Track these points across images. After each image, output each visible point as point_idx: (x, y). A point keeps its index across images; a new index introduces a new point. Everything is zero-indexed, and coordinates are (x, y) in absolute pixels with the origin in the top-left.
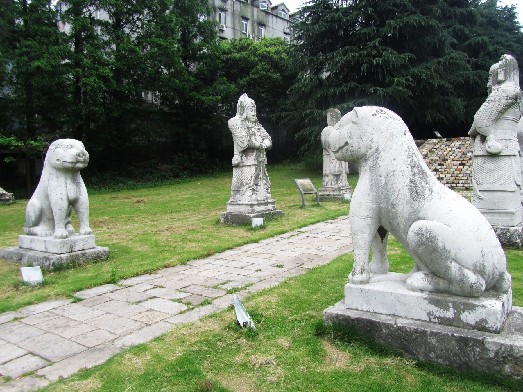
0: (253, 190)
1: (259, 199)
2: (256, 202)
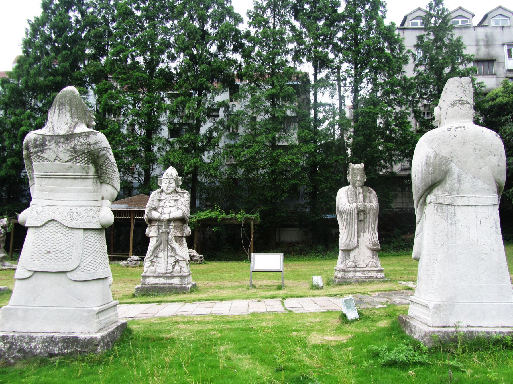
0: (152, 261)
1: (160, 271)
2: (152, 274)
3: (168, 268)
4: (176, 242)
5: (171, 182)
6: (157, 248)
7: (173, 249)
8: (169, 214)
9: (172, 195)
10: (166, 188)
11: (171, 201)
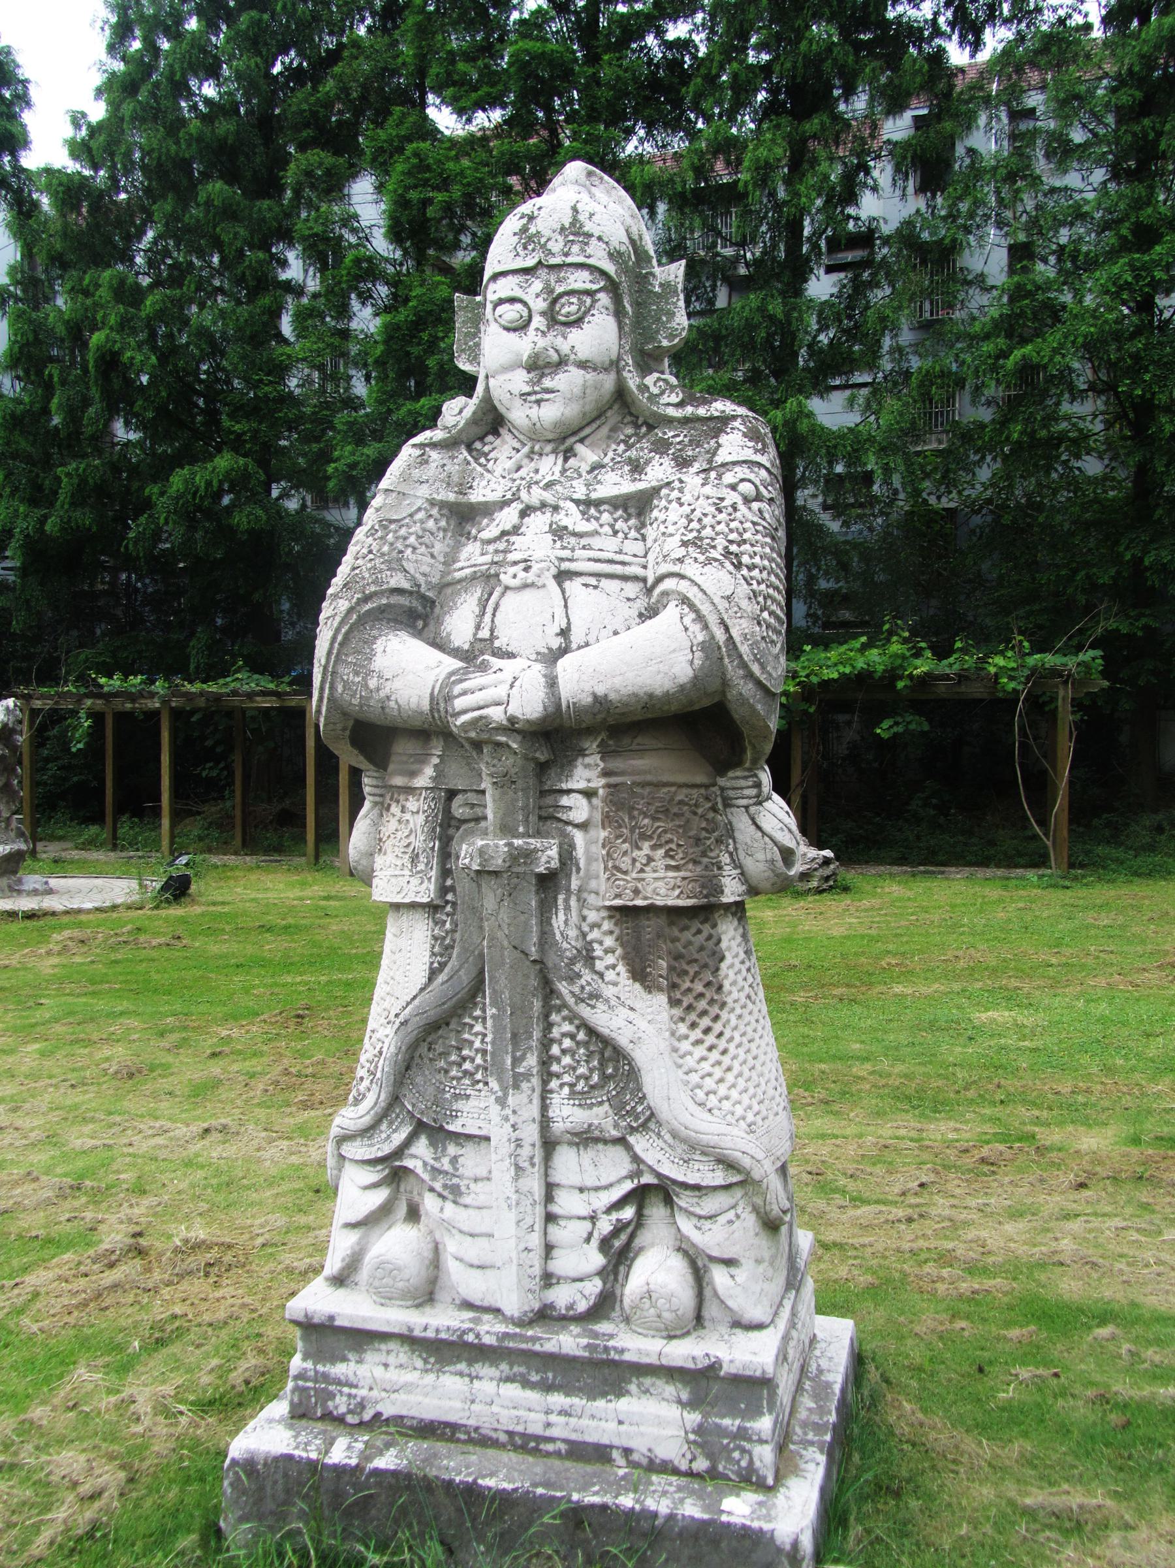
0: (394, 1172)
1: (472, 1285)
3: (562, 1264)
4: (639, 974)
5: (569, 308)
6: (432, 1036)
7: (612, 1064)
8: (552, 657)
9: (587, 455)
10: (520, 380)
11: (572, 518)
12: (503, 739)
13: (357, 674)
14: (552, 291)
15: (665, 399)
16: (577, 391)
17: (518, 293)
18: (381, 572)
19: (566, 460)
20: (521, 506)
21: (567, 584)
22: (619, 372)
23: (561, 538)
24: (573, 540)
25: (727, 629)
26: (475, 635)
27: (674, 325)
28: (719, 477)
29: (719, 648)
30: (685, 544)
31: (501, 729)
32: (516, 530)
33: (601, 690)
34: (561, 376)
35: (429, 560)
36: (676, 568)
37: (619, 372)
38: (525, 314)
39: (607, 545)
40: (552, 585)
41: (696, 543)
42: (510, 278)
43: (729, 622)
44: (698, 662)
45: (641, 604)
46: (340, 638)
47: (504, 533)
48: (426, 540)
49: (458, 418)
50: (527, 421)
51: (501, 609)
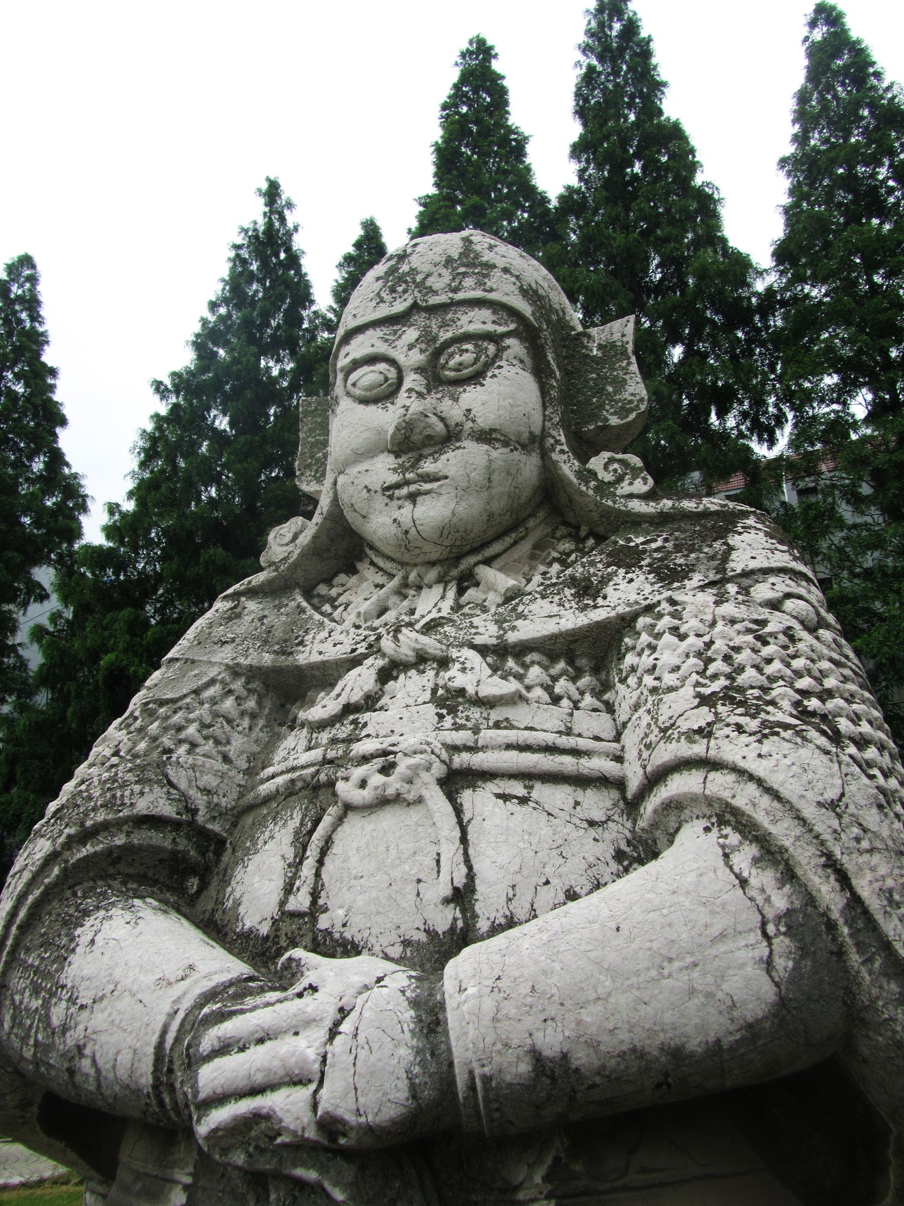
8: (433, 953)
10: (383, 469)
11: (473, 675)
12: (311, 1175)
13: (36, 991)
14: (435, 339)
15: (625, 488)
16: (477, 476)
17: (382, 348)
18: (123, 786)
19: (461, 591)
20: (381, 663)
21: (466, 797)
22: (544, 455)
23: (453, 711)
24: (475, 713)
25: (844, 879)
26: (283, 903)
27: (626, 396)
28: (745, 591)
29: (831, 926)
30: (705, 701)
31: (301, 1148)
32: (371, 702)
33: (551, 1042)
34: (450, 455)
35: (218, 765)
36: (698, 749)
37: (544, 455)
38: (392, 374)
39: (542, 720)
40: (437, 800)
41: (732, 695)
42: (370, 332)
43: (849, 863)
44: (784, 964)
45: (618, 832)
46: (22, 914)
47: (349, 709)
48: (216, 730)
49: (290, 548)
50: (393, 529)
51: (336, 849)
